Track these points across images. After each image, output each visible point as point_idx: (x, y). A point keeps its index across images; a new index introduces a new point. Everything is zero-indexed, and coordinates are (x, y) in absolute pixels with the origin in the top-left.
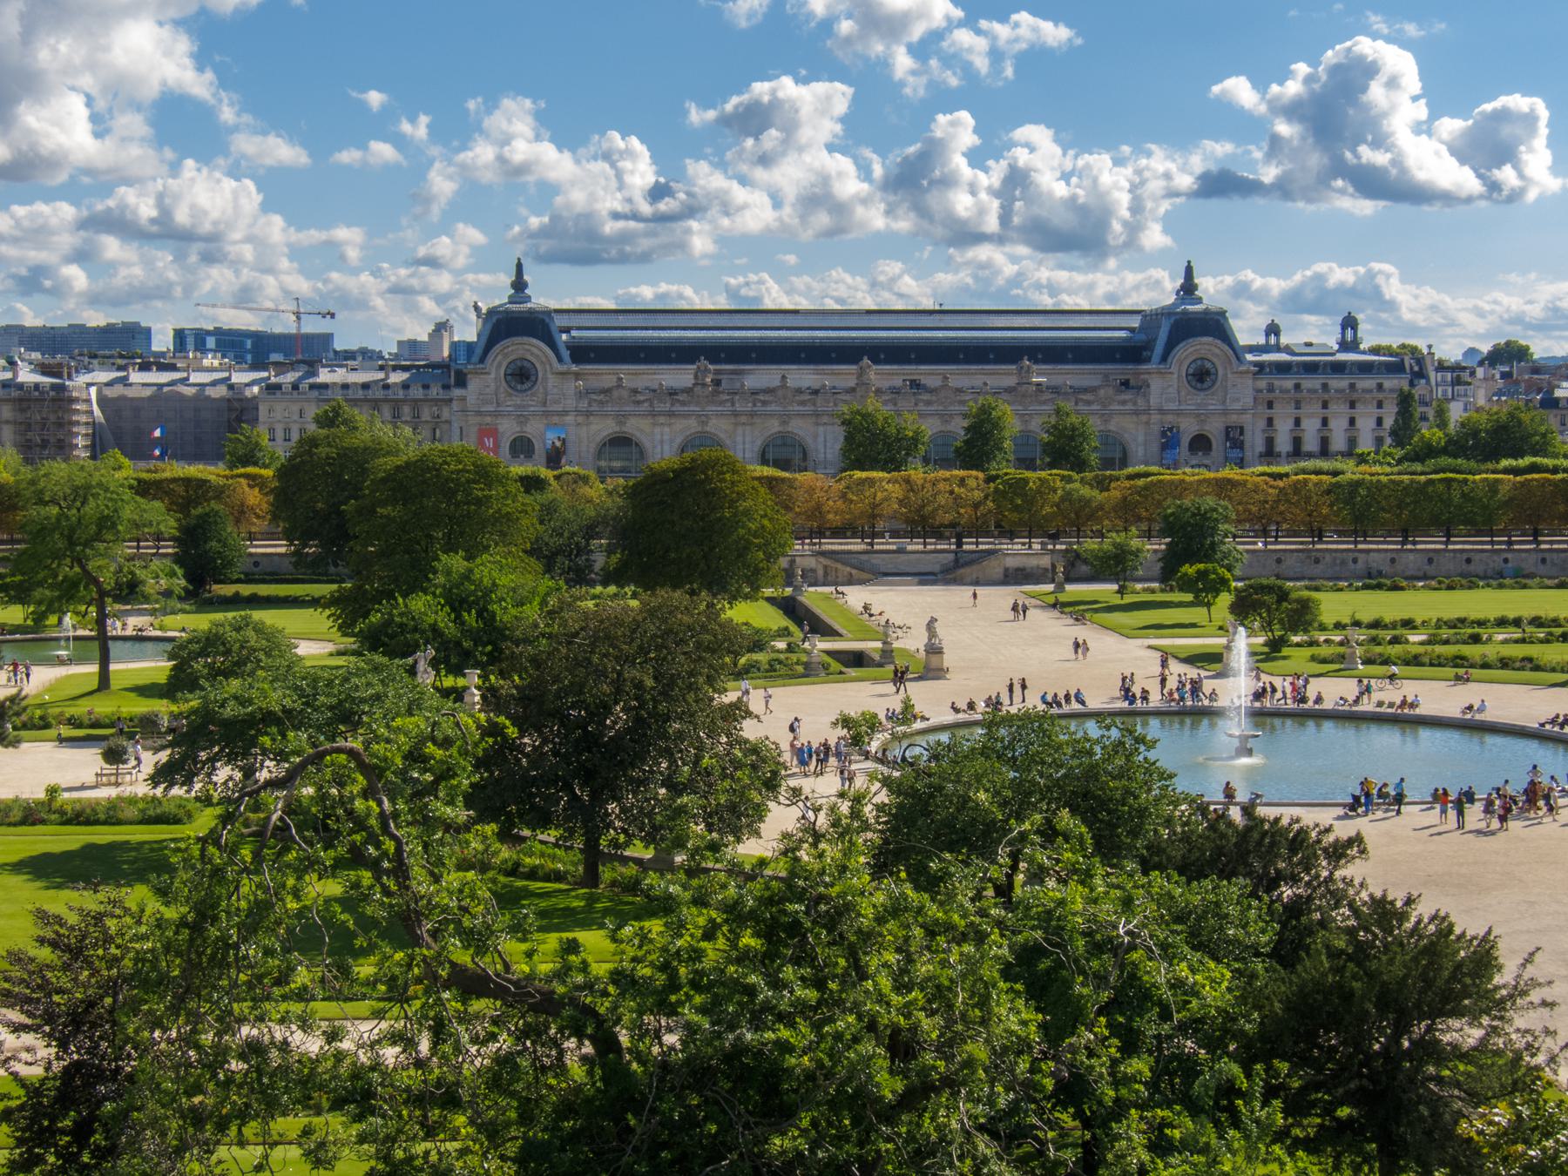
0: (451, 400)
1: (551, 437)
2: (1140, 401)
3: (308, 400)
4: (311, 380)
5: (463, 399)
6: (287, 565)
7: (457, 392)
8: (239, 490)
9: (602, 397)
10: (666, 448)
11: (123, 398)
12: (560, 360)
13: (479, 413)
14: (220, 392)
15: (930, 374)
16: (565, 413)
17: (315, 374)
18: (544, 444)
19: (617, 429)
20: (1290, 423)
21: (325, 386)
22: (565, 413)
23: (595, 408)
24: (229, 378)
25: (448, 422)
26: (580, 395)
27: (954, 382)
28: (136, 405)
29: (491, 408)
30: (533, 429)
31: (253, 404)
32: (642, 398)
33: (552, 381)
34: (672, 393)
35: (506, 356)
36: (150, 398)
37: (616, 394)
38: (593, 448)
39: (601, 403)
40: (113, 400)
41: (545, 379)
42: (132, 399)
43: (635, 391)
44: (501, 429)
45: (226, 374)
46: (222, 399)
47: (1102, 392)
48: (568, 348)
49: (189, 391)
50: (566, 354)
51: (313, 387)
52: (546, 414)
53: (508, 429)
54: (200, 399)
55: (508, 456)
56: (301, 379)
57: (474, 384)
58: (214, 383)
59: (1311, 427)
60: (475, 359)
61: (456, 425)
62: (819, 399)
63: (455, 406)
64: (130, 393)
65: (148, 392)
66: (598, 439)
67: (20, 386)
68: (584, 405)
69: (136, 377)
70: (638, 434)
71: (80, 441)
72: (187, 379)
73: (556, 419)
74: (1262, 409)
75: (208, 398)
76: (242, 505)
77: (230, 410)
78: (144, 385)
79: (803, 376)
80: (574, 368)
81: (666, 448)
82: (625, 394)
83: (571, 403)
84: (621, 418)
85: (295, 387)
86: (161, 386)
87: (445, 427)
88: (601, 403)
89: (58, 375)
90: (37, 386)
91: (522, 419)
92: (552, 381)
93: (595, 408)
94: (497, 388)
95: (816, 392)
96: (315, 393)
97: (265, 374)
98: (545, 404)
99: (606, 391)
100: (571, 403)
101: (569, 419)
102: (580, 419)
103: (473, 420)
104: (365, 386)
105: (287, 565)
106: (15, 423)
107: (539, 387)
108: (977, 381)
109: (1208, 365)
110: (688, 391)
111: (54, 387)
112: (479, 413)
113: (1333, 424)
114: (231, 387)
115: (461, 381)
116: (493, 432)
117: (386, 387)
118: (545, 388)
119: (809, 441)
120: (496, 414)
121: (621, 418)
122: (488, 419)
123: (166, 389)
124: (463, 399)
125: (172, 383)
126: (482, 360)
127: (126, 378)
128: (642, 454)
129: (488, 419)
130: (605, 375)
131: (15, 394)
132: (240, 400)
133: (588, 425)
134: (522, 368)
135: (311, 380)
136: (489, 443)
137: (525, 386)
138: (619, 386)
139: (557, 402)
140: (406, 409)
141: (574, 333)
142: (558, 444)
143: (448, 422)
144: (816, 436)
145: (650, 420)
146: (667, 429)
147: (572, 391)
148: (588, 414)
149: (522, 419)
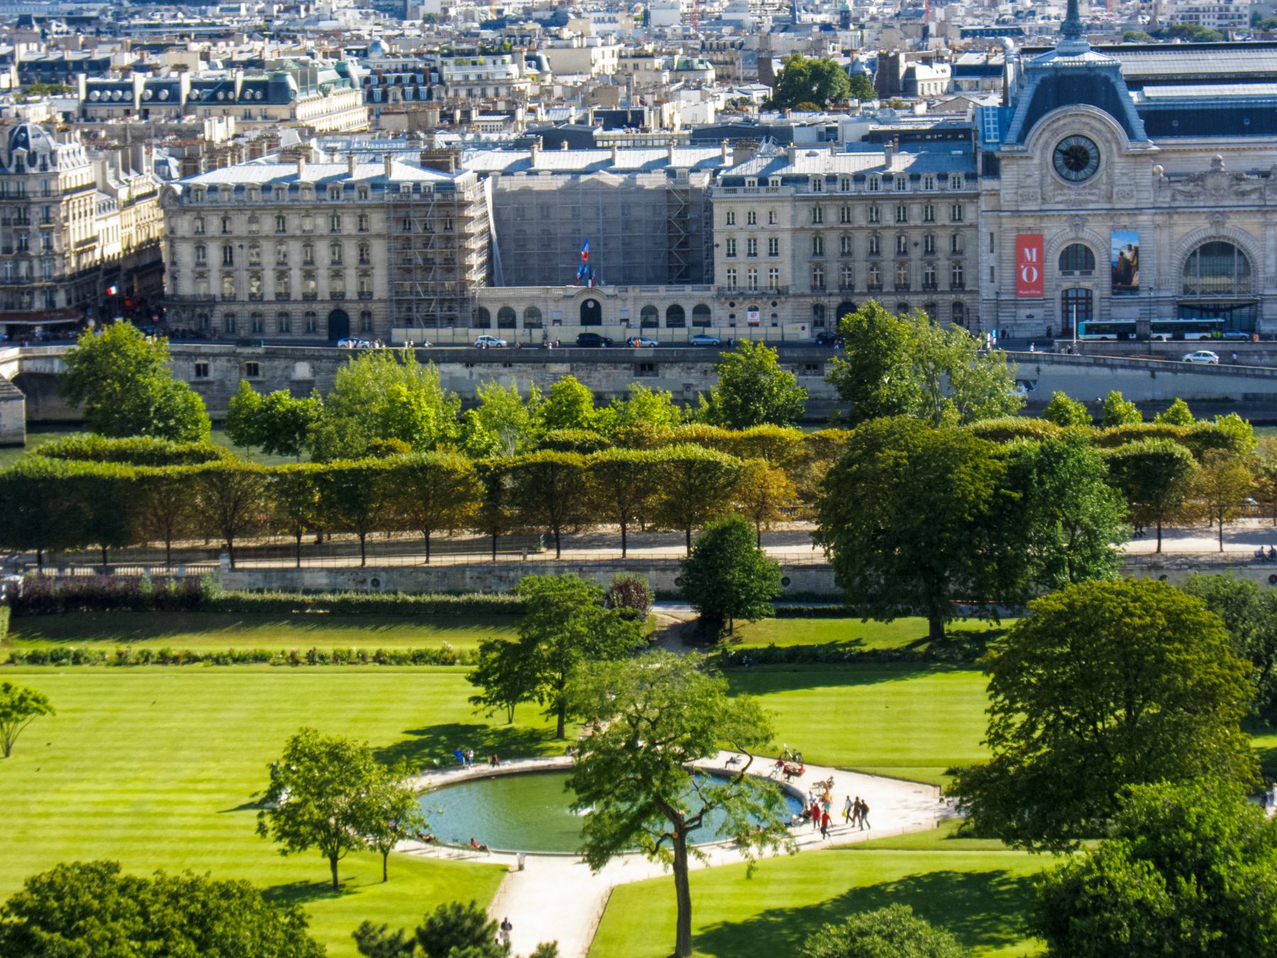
0: (977, 196)
1: (1119, 246)
3: (781, 200)
4: (784, 171)
5: (995, 194)
6: (828, 582)
7: (986, 184)
8: (758, 474)
9: (1190, 187)
11: (526, 192)
12: (1131, 135)
13: (1016, 213)
14: (657, 180)
16: (1139, 210)
17: (786, 160)
18: (1109, 258)
19: (1212, 232)
21: (802, 179)
22: (1139, 210)
23: (1180, 202)
24: (667, 160)
25: (974, 226)
26: (1159, 185)
28: (545, 201)
29: (1034, 206)
30: (1094, 234)
31: (704, 202)
32: (1248, 187)
33: (1120, 165)
35: (1055, 132)
36: (561, 191)
37: (1210, 182)
38: (1178, 259)
39: (1190, 195)
40: (514, 194)
41: (1110, 164)
42: (539, 193)
43: (1238, 178)
44: (1047, 235)
45: (662, 154)
46: (660, 191)
48: (1142, 114)
49: (615, 180)
50: (1138, 124)
51: (787, 180)
52: (1112, 212)
53: (1058, 235)
54: (630, 191)
55: (1058, 273)
56: (770, 168)
57: (1009, 172)
58: (648, 168)
60: (1012, 136)
61: (984, 231)
63: (984, 203)
64: (537, 184)
65: (560, 182)
66: (1185, 246)
67: (395, 187)
68: (1165, 199)
69: (544, 160)
70: (1242, 240)
71: (475, 260)
72: (610, 162)
73: (1125, 220)
75: (640, 189)
76: (764, 496)
77: (671, 205)
78: (555, 173)
82: (1224, 182)
83: (1147, 197)
84: (1218, 215)
85: (763, 181)
86: (575, 173)
87: (969, 233)
88: (1190, 195)
89: (442, 167)
90: (417, 186)
91: (1077, 221)
92: (1120, 165)
93: (1180, 202)
94: (1043, 177)
96: (790, 190)
97: (714, 152)
98: (1109, 198)
99: (1198, 179)
100: (1147, 197)
101: (1144, 219)
102: (1160, 219)
103: (1008, 223)
104: (859, 177)
105: (828, 582)
106: (388, 237)
107: (1101, 174)
111: (441, 187)
112: (1016, 213)
114: (671, 173)
115: (992, 168)
116: (1035, 240)
117: (888, 178)
118: (1110, 176)
120: (1041, 214)
121: (1218, 215)
122: (1029, 222)
123: (583, 178)
124: (995, 194)
125: (589, 170)
126: (1021, 139)
127: (529, 162)
128: (1247, 267)
129: (1029, 222)
131: (389, 197)
132: (686, 191)
133: (1171, 226)
134: (1081, 149)
135: (784, 171)
136: (1031, 255)
137: (1081, 174)
138: (1216, 172)
139: (1129, 196)
140: (916, 210)
141: (1150, 91)
142: (1128, 255)
143: (974, 226)
145: (1259, 219)
147: (1147, 180)
148: (1171, 211)
149: (1077, 221)
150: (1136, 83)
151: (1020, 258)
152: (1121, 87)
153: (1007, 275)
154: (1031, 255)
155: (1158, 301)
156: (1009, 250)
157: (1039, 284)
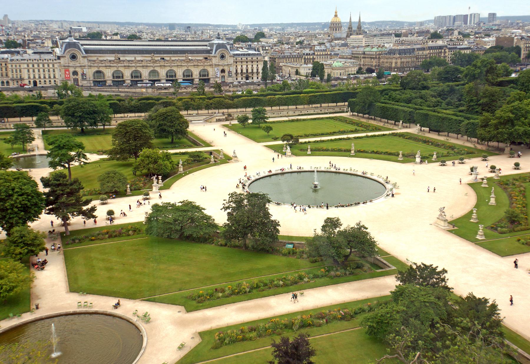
2: (210, 62)
10: (110, 73)
13: (64, 66)
15: (167, 57)
20: (240, 67)
27: (173, 59)
29: (67, 65)
33: (81, 59)
34: (110, 61)
37: (97, 62)
41: (80, 58)
44: (70, 69)
47: (203, 61)
53: (72, 70)
59: (244, 67)
62: (143, 63)
68: (89, 64)
74: (235, 64)
79: (139, 57)
80: (86, 55)
81: (110, 73)
93: (92, 65)
94: (68, 60)
95: (142, 61)
102: (89, 67)
108: (177, 58)
109: (224, 55)
110: (113, 61)
113: (248, 66)
116: (68, 71)
119: (142, 71)
129: (67, 67)
130: (94, 57)
136: (67, 73)
141: (85, 46)
144: (143, 71)
146: (109, 69)
150: (82, 45)
151: (65, 73)
152: (80, 46)
153: (63, 76)
154: (67, 73)
155: (90, 80)
156: (63, 71)
157: (69, 77)
